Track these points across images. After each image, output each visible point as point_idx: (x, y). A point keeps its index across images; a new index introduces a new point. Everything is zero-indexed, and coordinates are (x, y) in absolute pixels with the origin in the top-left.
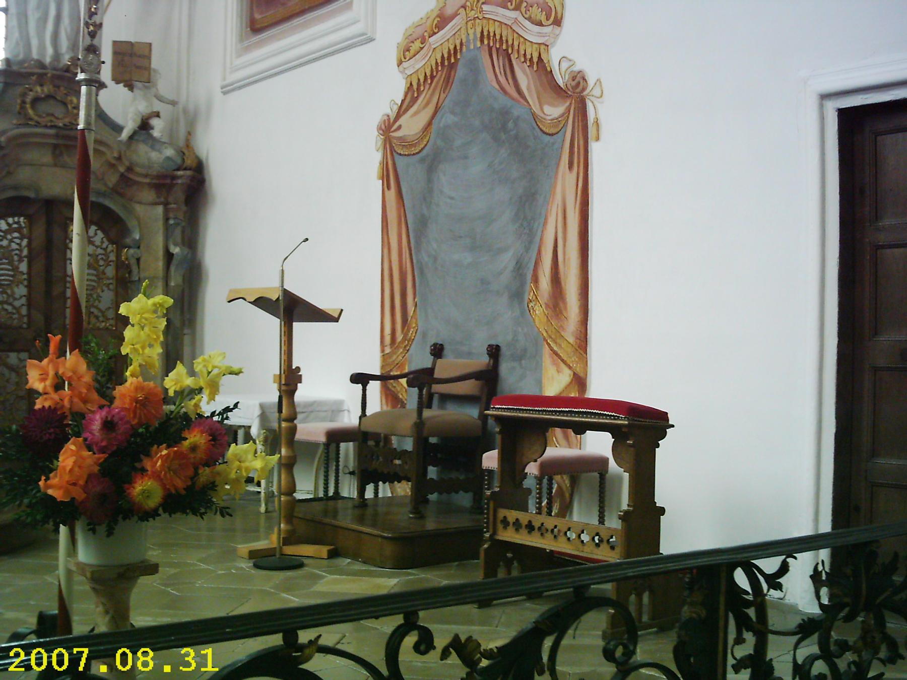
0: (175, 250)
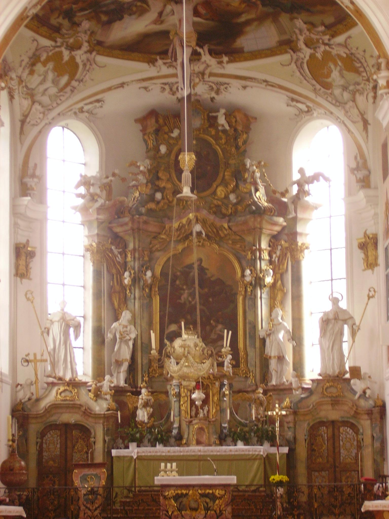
0: (375, 435)
